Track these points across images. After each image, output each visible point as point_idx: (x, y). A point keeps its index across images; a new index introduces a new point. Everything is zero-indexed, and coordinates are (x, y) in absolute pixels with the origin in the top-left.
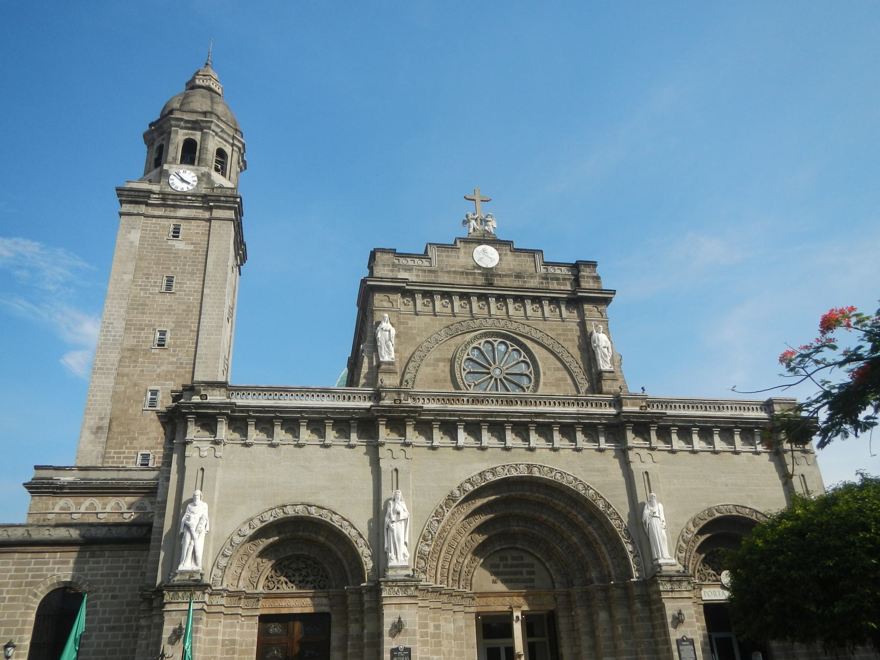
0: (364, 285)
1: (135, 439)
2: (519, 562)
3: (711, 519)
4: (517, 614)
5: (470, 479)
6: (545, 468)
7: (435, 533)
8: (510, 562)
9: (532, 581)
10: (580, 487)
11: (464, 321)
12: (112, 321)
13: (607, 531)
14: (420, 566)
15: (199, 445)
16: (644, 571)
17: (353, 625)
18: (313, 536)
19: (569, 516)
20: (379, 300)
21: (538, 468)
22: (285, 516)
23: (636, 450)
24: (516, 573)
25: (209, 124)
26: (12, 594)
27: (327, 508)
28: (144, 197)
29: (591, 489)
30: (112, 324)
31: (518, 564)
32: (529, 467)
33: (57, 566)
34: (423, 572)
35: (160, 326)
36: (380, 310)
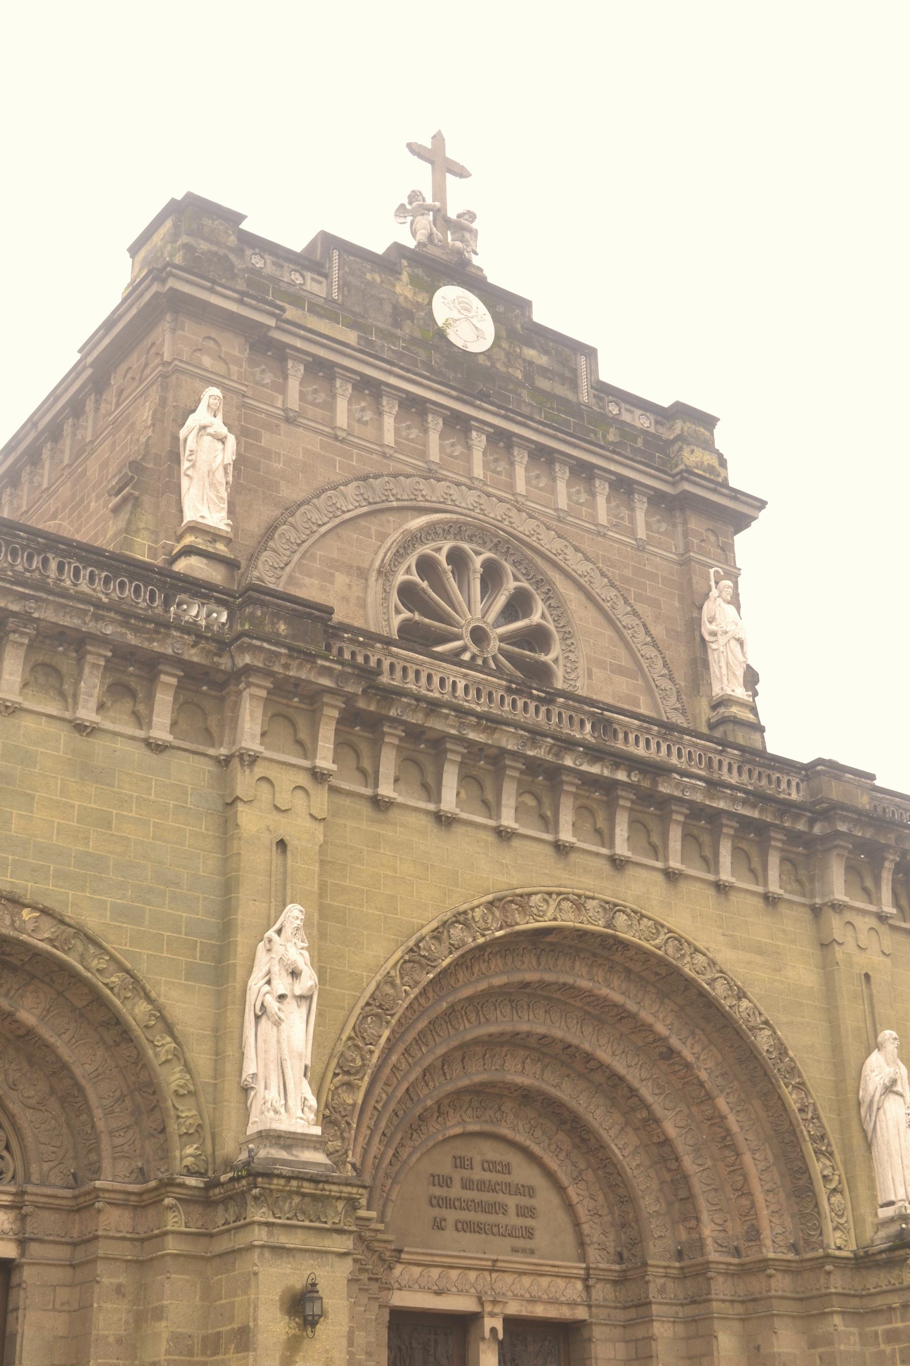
0: (155, 288)
2: (500, 1178)
4: (493, 1323)
5: (465, 913)
6: (645, 920)
8: (478, 1174)
9: (529, 1233)
11: (408, 476)
17: (109, 1306)
21: (628, 915)
23: (849, 916)
27: (72, 922)
36: (193, 375)
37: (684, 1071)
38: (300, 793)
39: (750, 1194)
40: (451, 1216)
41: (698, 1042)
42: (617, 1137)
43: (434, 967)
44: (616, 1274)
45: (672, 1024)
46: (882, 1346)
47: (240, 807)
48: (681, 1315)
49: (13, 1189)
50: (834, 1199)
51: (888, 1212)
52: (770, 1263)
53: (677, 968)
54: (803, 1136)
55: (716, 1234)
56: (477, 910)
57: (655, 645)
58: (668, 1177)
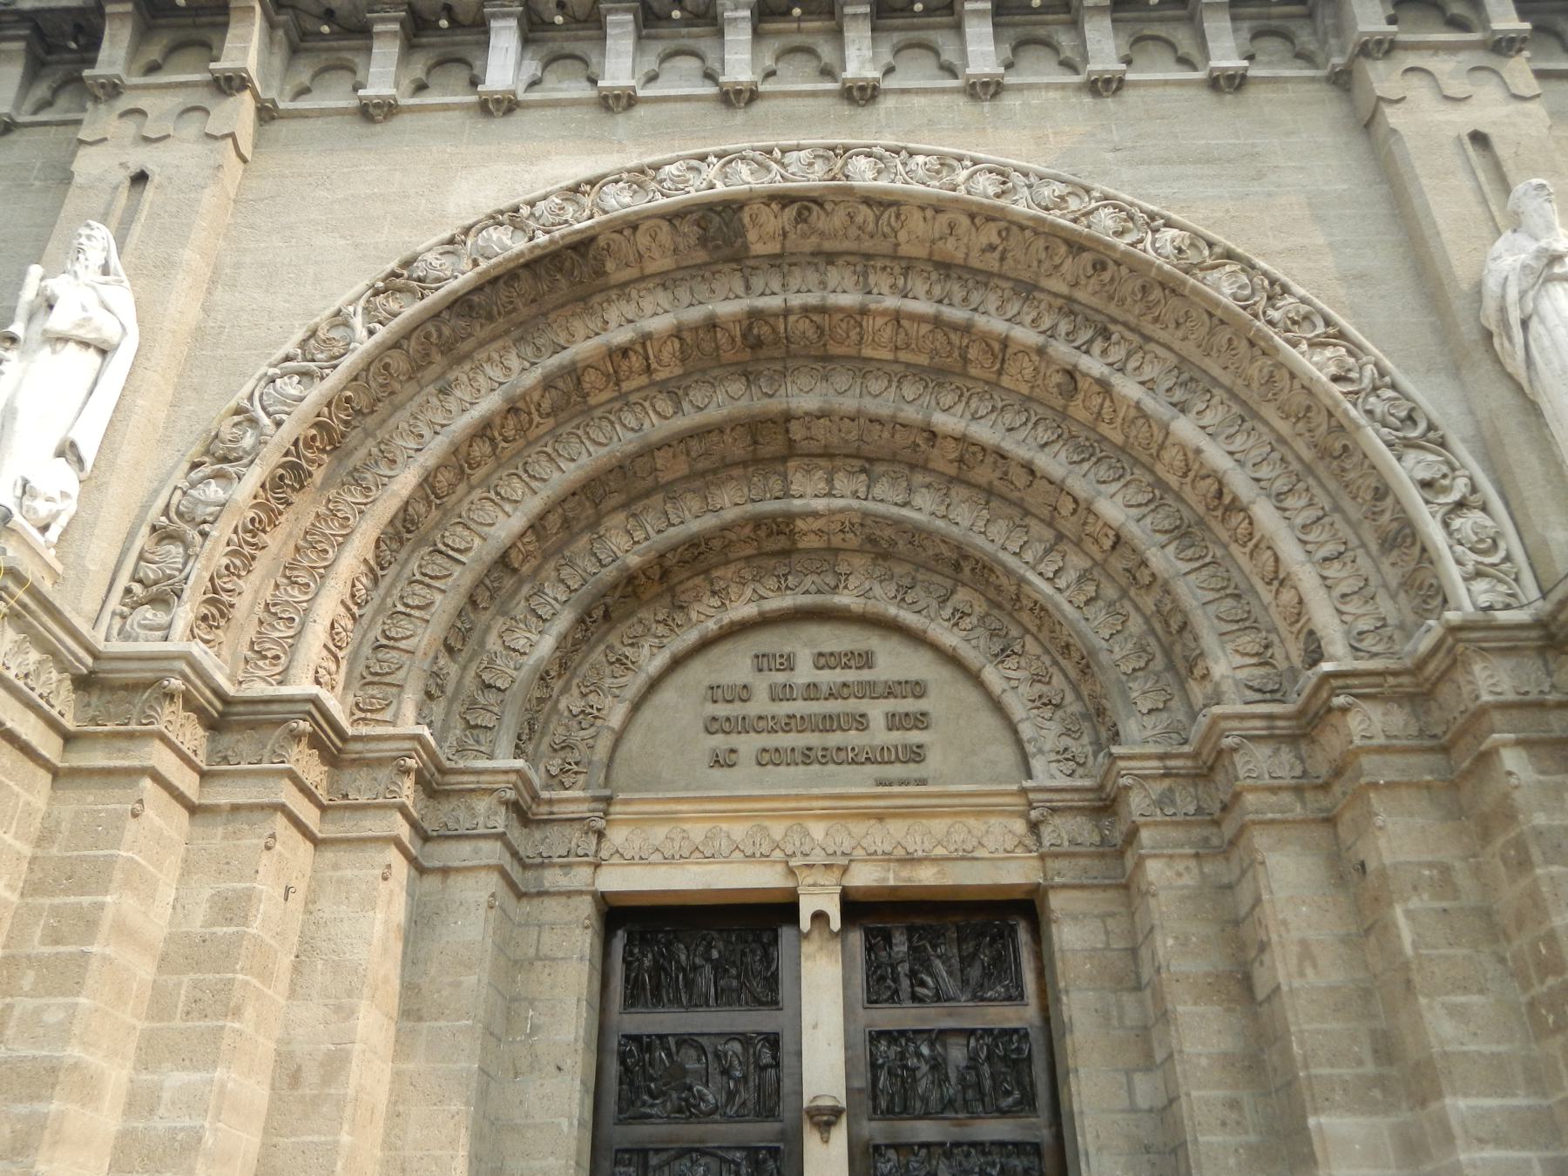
2: (851, 676)
5: (517, 210)
6: (920, 159)
7: (279, 424)
8: (804, 673)
9: (916, 754)
10: (1105, 222)
13: (1281, 440)
14: (150, 572)
16: (1527, 577)
19: (1077, 410)
21: (881, 159)
24: (829, 723)
29: (1167, 225)
31: (845, 685)
34: (160, 601)
37: (1107, 403)
38: (196, 115)
40: (747, 744)
41: (1118, 343)
42: (1041, 560)
43: (437, 289)
44: (1091, 796)
45: (1054, 327)
48: (1215, 841)
50: (1466, 523)
52: (1334, 683)
53: (1002, 209)
54: (1352, 420)
55: (1242, 674)
56: (541, 205)
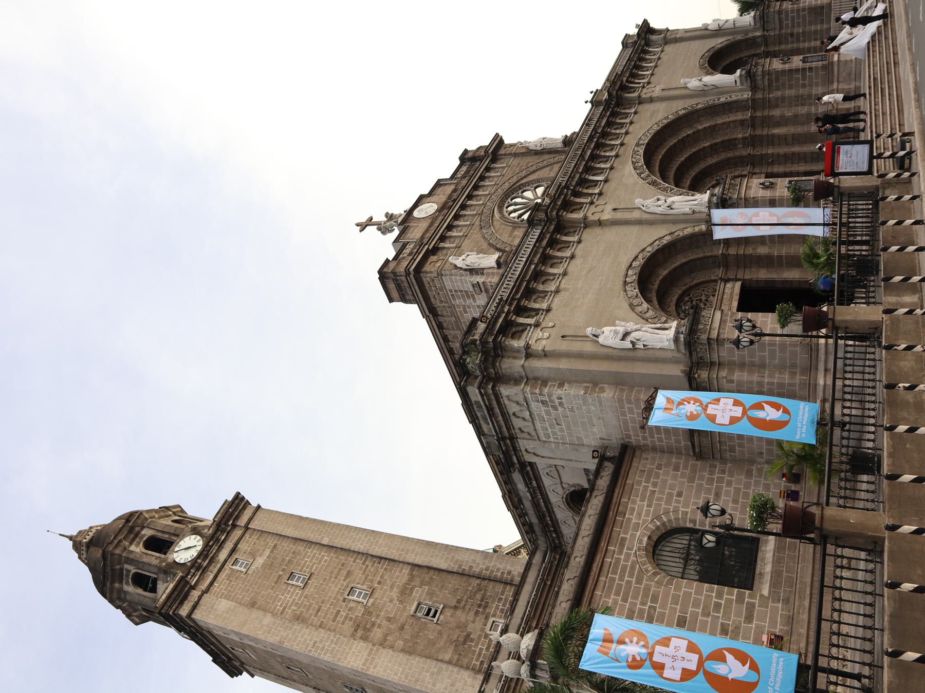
0: (412, 276)
1: (468, 635)
3: (708, 67)
11: (481, 218)
12: (312, 643)
15: (535, 339)
18: (661, 278)
20: (432, 267)
22: (636, 282)
25: (142, 517)
26: (648, 599)
28: (184, 586)
30: (315, 642)
32: (638, 145)
33: (625, 551)
35: (342, 594)
39: (730, 122)
46: (780, 84)
47: (602, 219)
49: (719, 281)
50: (733, 97)
51: (738, 81)
57: (543, 161)
58: (722, 149)
